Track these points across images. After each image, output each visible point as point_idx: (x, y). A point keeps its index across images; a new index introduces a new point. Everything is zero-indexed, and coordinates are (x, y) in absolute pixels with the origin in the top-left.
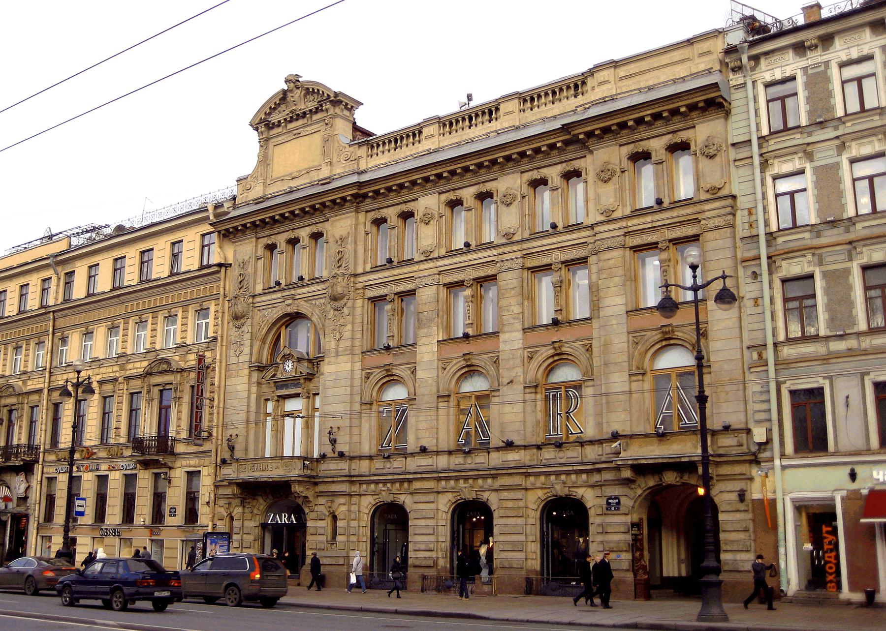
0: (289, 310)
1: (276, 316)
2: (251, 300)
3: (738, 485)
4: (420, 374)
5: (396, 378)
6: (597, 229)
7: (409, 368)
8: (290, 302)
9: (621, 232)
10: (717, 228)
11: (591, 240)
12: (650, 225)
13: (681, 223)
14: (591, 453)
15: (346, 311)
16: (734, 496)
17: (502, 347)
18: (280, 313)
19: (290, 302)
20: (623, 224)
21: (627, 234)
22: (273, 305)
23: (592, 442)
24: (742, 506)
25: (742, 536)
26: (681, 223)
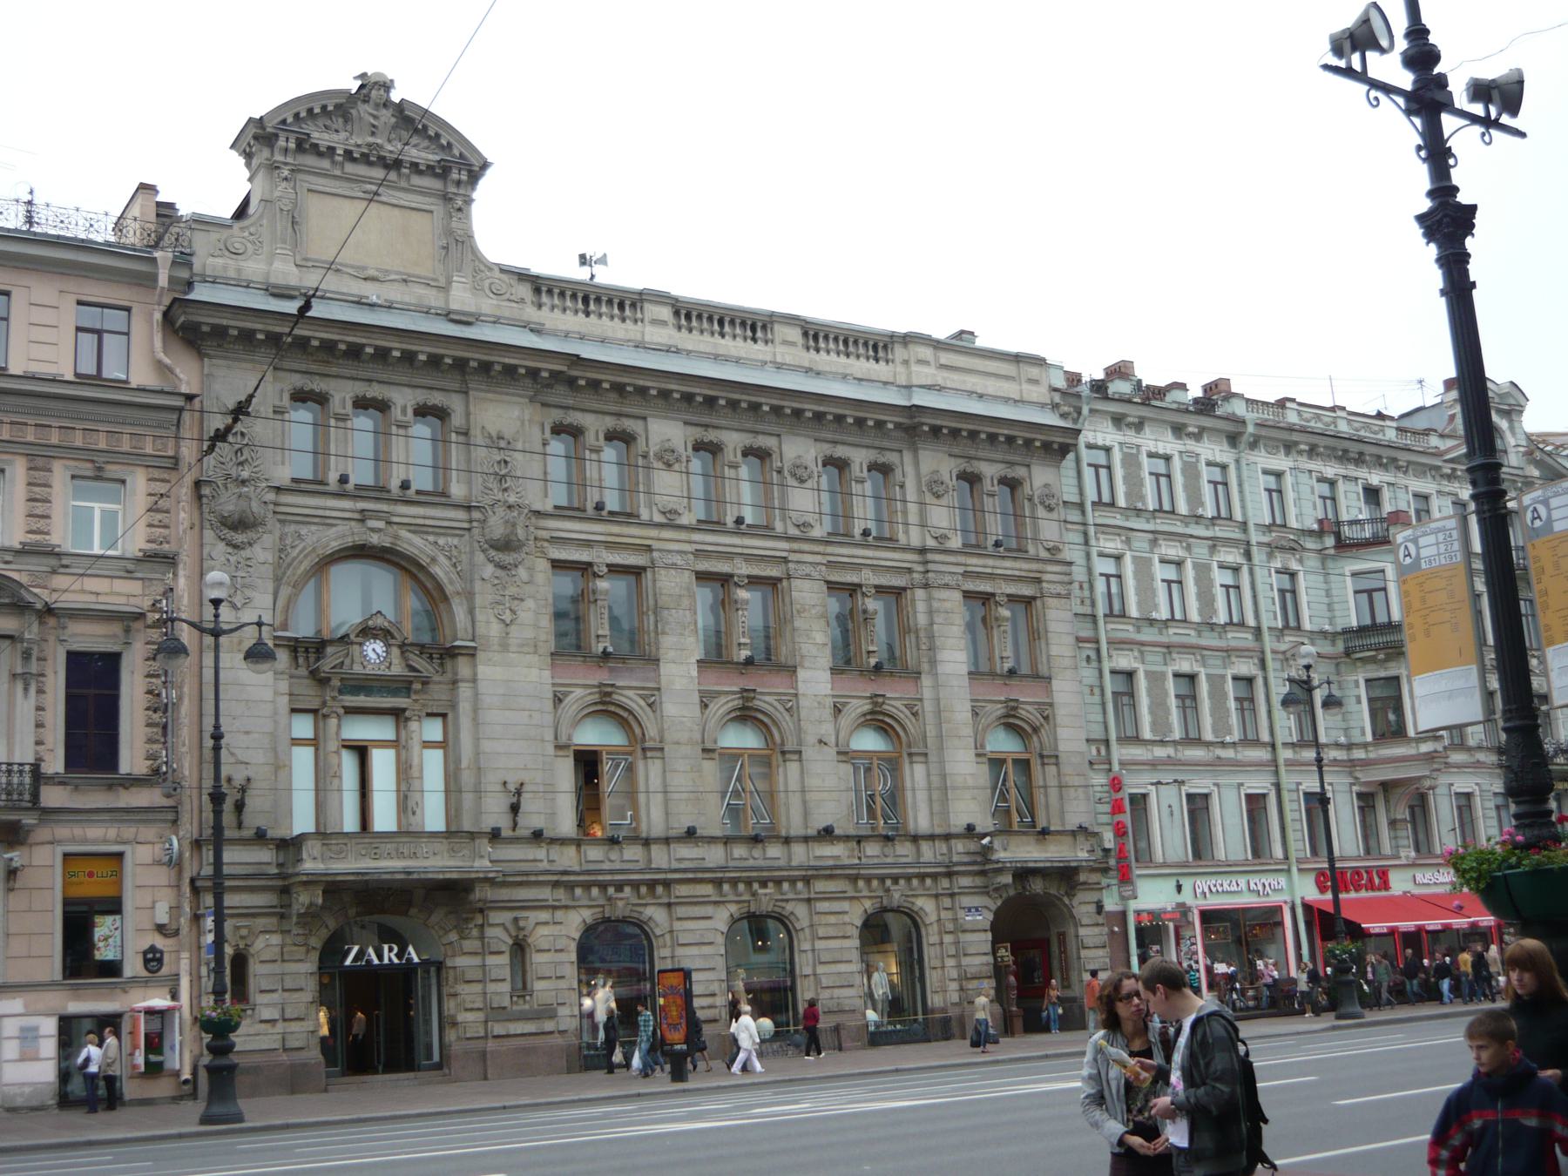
0: (375, 539)
1: (335, 545)
2: (271, 496)
3: (1092, 896)
4: (670, 708)
5: (612, 708)
6: (930, 556)
7: (643, 697)
8: (381, 524)
9: (960, 570)
10: (1059, 596)
11: (920, 568)
12: (989, 570)
13: (1019, 579)
14: (928, 852)
15: (522, 572)
16: (1092, 908)
17: (802, 688)
18: (349, 541)
19: (381, 524)
20: (961, 559)
21: (966, 574)
22: (325, 521)
23: (932, 837)
24: (1100, 920)
25: (1101, 952)
26: (1019, 579)
